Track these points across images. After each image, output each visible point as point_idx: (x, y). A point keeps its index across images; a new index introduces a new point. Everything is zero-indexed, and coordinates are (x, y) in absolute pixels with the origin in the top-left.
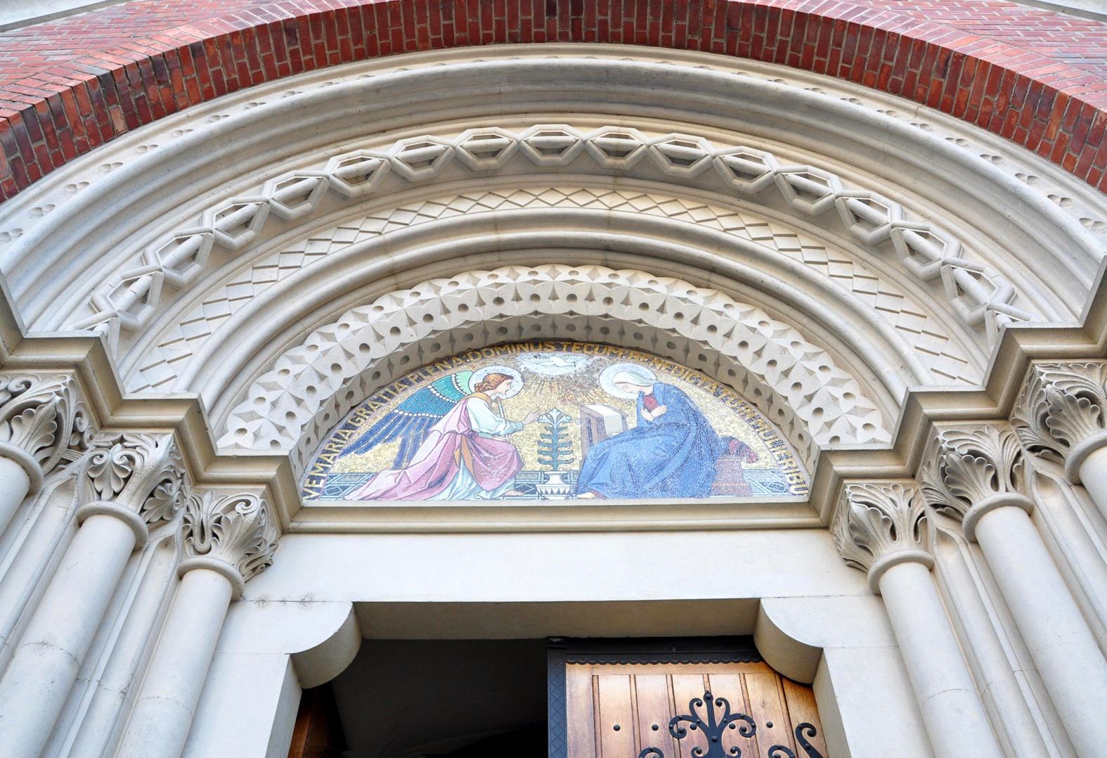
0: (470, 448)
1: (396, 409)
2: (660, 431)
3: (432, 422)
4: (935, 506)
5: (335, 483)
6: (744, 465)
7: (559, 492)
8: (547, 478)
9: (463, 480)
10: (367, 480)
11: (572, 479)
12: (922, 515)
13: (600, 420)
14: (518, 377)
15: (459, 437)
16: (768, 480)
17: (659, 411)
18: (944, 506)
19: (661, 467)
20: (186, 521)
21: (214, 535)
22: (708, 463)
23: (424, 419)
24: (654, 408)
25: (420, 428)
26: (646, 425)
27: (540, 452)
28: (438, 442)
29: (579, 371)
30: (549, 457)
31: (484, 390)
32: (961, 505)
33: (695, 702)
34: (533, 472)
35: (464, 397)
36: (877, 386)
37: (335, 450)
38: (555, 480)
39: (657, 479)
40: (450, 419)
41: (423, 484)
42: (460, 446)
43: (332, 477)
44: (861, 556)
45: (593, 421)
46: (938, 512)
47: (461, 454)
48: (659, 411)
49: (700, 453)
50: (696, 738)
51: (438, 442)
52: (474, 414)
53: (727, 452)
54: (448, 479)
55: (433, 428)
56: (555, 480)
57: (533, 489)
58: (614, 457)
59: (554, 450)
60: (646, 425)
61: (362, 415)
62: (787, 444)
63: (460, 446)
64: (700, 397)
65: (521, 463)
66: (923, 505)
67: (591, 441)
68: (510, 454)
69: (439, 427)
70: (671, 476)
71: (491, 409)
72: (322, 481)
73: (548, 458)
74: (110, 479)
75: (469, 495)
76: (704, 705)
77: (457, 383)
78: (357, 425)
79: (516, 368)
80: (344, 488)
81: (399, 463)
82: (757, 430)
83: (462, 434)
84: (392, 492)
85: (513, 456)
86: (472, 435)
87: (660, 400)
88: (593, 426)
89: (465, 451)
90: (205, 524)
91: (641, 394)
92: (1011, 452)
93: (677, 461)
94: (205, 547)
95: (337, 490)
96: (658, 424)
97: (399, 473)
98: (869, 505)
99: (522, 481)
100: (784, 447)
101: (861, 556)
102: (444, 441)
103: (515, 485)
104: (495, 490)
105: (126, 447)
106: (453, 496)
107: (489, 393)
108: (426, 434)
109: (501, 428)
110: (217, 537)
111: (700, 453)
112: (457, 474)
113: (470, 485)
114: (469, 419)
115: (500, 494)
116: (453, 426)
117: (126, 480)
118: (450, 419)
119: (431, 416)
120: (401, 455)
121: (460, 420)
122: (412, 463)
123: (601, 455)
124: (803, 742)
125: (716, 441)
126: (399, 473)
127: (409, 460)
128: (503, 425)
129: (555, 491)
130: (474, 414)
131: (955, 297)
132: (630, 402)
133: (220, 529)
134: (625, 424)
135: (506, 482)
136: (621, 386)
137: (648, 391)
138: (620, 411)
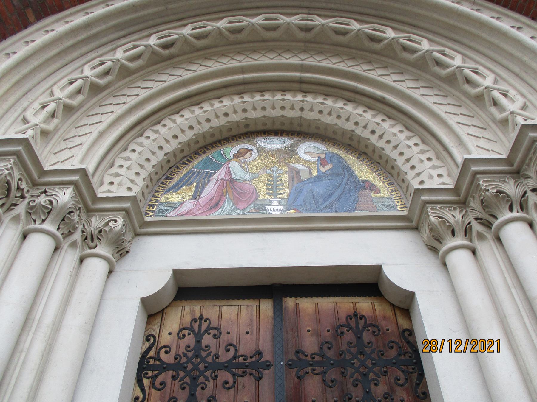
0: (231, 188)
1: (193, 168)
2: (329, 177)
3: (212, 174)
4: (476, 219)
5: (162, 207)
6: (373, 195)
7: (277, 210)
8: (271, 202)
9: (228, 204)
10: (179, 206)
11: (283, 202)
12: (469, 223)
13: (298, 172)
14: (255, 151)
15: (225, 182)
16: (386, 203)
17: (328, 167)
18: (481, 219)
19: (330, 196)
20: (83, 232)
21: (99, 238)
22: (354, 194)
23: (207, 173)
24: (326, 165)
25: (205, 178)
26: (322, 174)
28: (215, 185)
30: (272, 192)
32: (491, 219)
33: (349, 317)
34: (263, 200)
35: (228, 161)
36: (444, 153)
37: (161, 191)
38: (275, 203)
39: (327, 203)
40: (221, 172)
43: (160, 205)
44: (436, 244)
46: (478, 222)
48: (328, 167)
49: (350, 189)
50: (349, 336)
51: (215, 185)
52: (233, 170)
53: (364, 188)
54: (220, 204)
55: (212, 178)
56: (275, 203)
57: (264, 208)
60: (322, 174)
61: (175, 171)
62: (396, 184)
63: (226, 187)
64: (350, 159)
66: (470, 218)
68: (252, 190)
69: (215, 177)
70: (335, 201)
71: (242, 167)
72: (155, 207)
73: (271, 192)
74: (39, 213)
75: (231, 212)
76: (353, 319)
77: (224, 154)
78: (173, 177)
79: (254, 145)
80: (167, 210)
81: (195, 197)
82: (380, 177)
83: (227, 180)
85: (253, 191)
86: (232, 181)
88: (295, 174)
90: (93, 233)
91: (319, 158)
92: (520, 191)
93: (338, 193)
94: (94, 244)
95: (163, 211)
97: (195, 202)
98: (440, 218)
99: (258, 204)
100: (394, 185)
101: (436, 244)
102: (218, 184)
103: (255, 206)
104: (244, 209)
105: (47, 196)
106: (224, 212)
108: (209, 181)
109: (247, 177)
110: (100, 240)
111: (350, 189)
112: (225, 201)
113: (232, 207)
115: (247, 211)
116: (222, 176)
117: (49, 213)
118: (221, 172)
119: (211, 171)
120: (196, 192)
121: (226, 173)
123: (299, 190)
124: (405, 338)
125: (358, 182)
126: (195, 202)
128: (248, 175)
129: (275, 209)
130: (233, 170)
131: (492, 106)
132: (313, 162)
133: (101, 235)
135: (250, 205)
136: (309, 154)
137: (323, 156)
138: (308, 167)
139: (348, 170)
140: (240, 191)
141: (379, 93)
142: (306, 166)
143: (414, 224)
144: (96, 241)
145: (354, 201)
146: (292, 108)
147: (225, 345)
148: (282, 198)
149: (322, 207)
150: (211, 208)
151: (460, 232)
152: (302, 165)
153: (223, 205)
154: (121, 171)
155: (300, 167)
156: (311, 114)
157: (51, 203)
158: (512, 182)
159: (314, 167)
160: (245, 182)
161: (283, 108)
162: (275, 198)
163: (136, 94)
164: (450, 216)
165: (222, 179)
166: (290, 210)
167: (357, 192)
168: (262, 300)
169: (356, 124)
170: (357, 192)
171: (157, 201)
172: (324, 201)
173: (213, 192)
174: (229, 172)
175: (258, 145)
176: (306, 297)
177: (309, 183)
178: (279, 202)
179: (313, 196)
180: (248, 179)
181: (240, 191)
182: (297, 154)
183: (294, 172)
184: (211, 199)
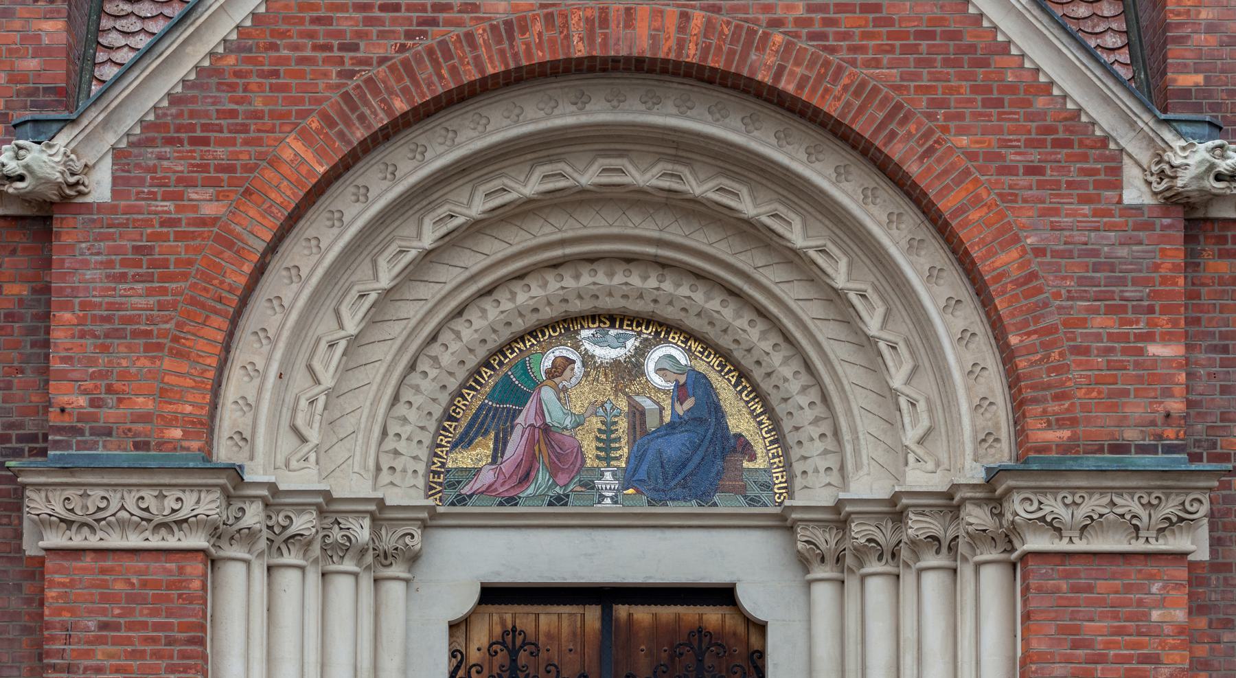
2: (688, 427)
5: (451, 477)
6: (746, 464)
8: (602, 475)
11: (620, 474)
13: (643, 413)
14: (578, 364)
15: (537, 430)
17: (689, 403)
20: (374, 549)
22: (719, 462)
27: (598, 448)
29: (628, 354)
31: (554, 377)
34: (592, 469)
35: (537, 385)
38: (608, 476)
39: (680, 476)
41: (515, 479)
42: (538, 441)
43: (448, 472)
45: (637, 414)
47: (540, 450)
48: (689, 403)
53: (734, 450)
54: (533, 474)
55: (517, 421)
56: (608, 476)
58: (650, 456)
59: (608, 449)
60: (677, 420)
65: (584, 461)
67: (635, 437)
68: (575, 450)
69: (520, 419)
70: (691, 474)
71: (559, 399)
73: (602, 454)
79: (576, 347)
83: (539, 428)
84: (494, 487)
86: (546, 429)
87: (691, 391)
88: (637, 414)
89: (543, 447)
93: (696, 459)
96: (686, 418)
99: (585, 477)
103: (580, 481)
104: (566, 486)
105: (341, 529)
107: (557, 380)
108: (513, 427)
109: (568, 422)
114: (543, 411)
117: (347, 550)
120: (495, 450)
122: (505, 458)
125: (728, 439)
127: (503, 454)
128: (569, 419)
129: (608, 487)
132: (665, 392)
134: (661, 417)
135: (573, 478)
137: (682, 379)
138: (658, 404)
139: (717, 411)
140: (559, 451)
141: (773, 309)
142: (654, 401)
143: (788, 523)
144: (390, 559)
145: (717, 475)
146: (641, 296)
147: (544, 665)
148: (618, 467)
149: (672, 484)
150: (520, 482)
151: (831, 560)
152: (650, 398)
153: (536, 478)
154: (402, 446)
155: (647, 404)
156: (670, 309)
157: (349, 539)
158: (890, 525)
159: (667, 404)
160: (566, 433)
161: (625, 296)
162: (608, 466)
163: (406, 316)
164: (823, 540)
165: (531, 425)
166: (628, 489)
167: (723, 459)
168: (587, 606)
169: (736, 341)
170: (723, 459)
171: (443, 465)
172: (675, 475)
173: (521, 449)
174: (540, 412)
175: (583, 348)
176: (643, 604)
177: (658, 437)
178: (614, 474)
179: (662, 463)
180: (569, 426)
181: (559, 451)
182: (643, 374)
183: (637, 414)
184: (519, 465)
